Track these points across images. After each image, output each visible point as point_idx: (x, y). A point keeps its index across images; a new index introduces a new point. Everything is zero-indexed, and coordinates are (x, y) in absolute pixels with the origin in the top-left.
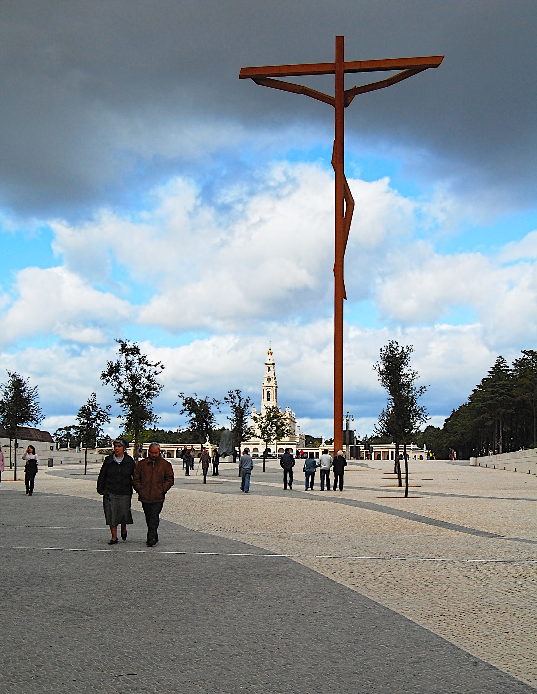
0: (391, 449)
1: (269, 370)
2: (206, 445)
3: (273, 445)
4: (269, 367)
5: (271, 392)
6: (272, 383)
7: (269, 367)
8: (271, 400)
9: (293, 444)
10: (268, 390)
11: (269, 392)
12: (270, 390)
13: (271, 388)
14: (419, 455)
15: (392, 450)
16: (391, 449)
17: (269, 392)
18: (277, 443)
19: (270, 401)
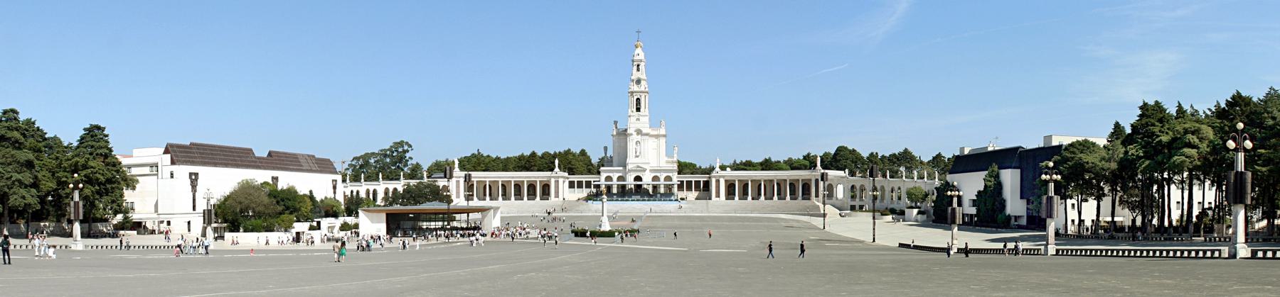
7: (638, 66)
10: (635, 98)
11: (638, 100)
12: (639, 97)
17: (638, 100)
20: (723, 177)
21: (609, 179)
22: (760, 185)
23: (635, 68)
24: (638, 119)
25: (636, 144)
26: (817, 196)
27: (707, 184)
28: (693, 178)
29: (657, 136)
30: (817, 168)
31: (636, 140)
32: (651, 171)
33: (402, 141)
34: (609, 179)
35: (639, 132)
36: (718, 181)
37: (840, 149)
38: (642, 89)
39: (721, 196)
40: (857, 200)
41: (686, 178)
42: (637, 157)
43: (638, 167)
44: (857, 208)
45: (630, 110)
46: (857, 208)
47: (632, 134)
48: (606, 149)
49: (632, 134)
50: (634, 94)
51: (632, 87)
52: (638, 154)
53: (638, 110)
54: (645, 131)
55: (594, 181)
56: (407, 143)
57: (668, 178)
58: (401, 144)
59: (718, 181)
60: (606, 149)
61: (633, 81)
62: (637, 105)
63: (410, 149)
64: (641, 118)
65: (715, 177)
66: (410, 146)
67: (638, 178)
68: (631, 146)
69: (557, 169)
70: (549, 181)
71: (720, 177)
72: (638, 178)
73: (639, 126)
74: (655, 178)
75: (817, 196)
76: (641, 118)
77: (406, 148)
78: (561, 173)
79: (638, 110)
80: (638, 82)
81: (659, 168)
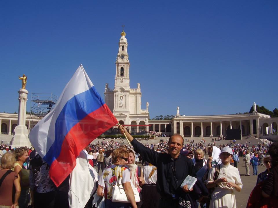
7: (123, 47)
12: (123, 66)
13: (124, 64)
19: (123, 76)
20: (183, 120)
23: (120, 48)
24: (122, 82)
25: (120, 98)
26: (255, 132)
29: (135, 94)
30: (254, 112)
32: (131, 117)
35: (123, 90)
36: (178, 124)
38: (125, 61)
42: (121, 107)
43: (122, 114)
45: (116, 75)
47: (117, 92)
50: (120, 64)
51: (118, 60)
52: (121, 105)
53: (122, 75)
54: (126, 90)
57: (142, 123)
61: (119, 56)
62: (121, 72)
64: (124, 80)
65: (176, 120)
68: (117, 100)
71: (180, 120)
73: (122, 85)
74: (134, 123)
75: (255, 132)
76: (124, 80)
80: (123, 57)
81: (136, 116)
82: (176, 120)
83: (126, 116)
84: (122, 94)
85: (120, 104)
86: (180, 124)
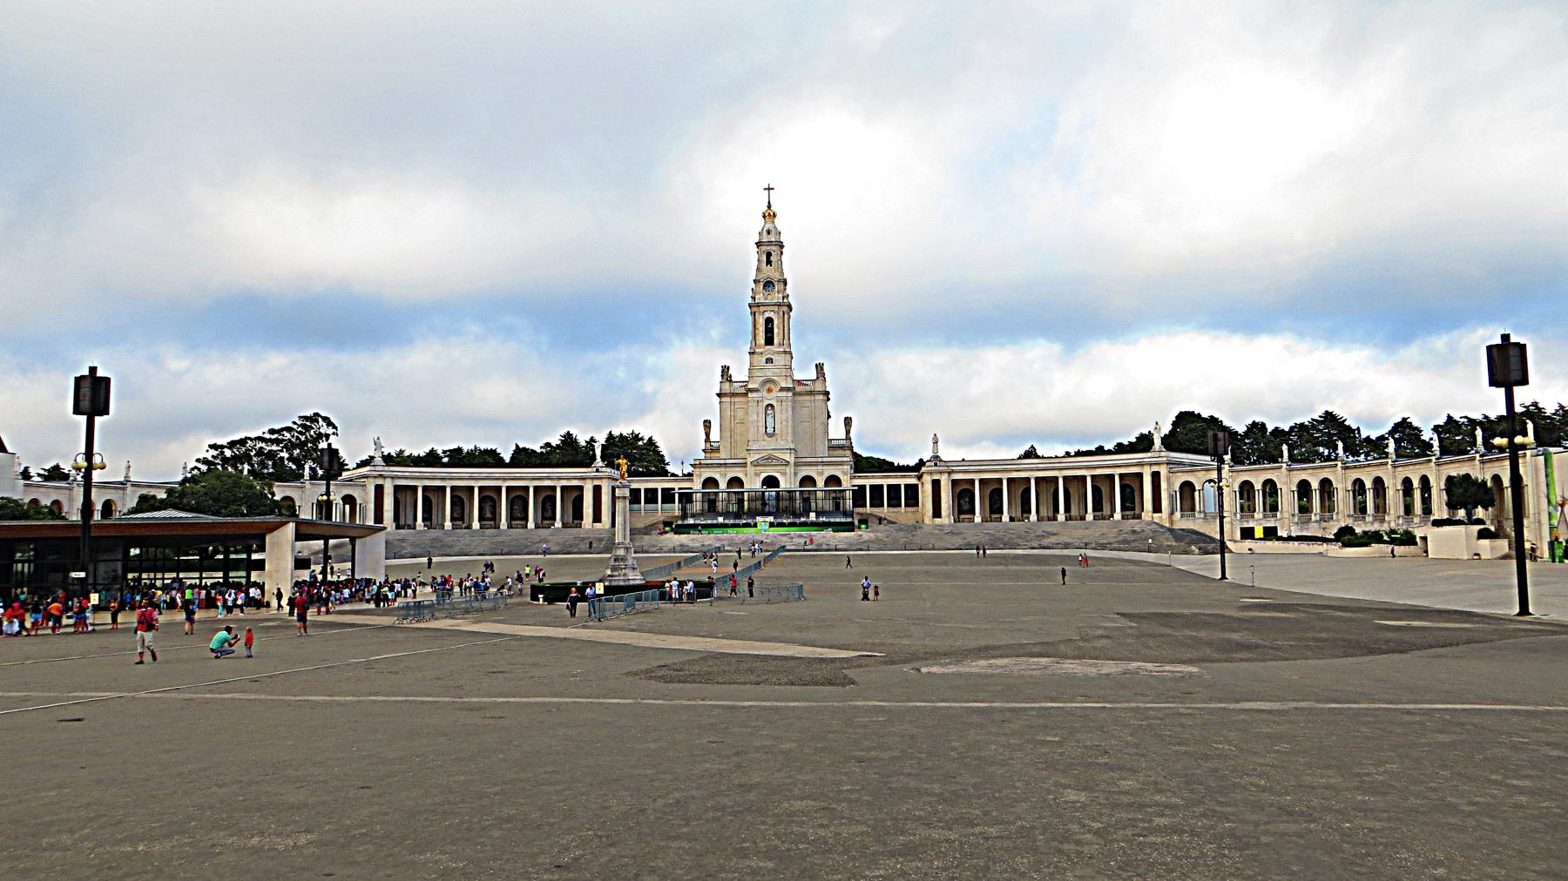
0: (1151, 464)
1: (769, 262)
2: (595, 469)
3: (784, 467)
4: (769, 255)
5: (776, 323)
6: (776, 297)
7: (769, 255)
8: (776, 341)
9: (842, 463)
10: (767, 315)
11: (769, 321)
12: (771, 315)
13: (776, 308)
14: (1296, 481)
15: (1155, 469)
16: (1151, 464)
17: (769, 321)
18: (796, 464)
19: (772, 344)
21: (710, 482)
22: (1028, 490)
24: (769, 361)
25: (768, 406)
27: (912, 491)
28: (885, 481)
31: (767, 402)
33: (317, 415)
34: (710, 482)
36: (936, 485)
37: (1184, 418)
39: (944, 513)
40: (1258, 515)
41: (868, 481)
42: (771, 436)
44: (1259, 533)
46: (1259, 533)
48: (707, 424)
49: (756, 390)
52: (770, 430)
53: (769, 341)
55: (680, 489)
56: (326, 419)
58: (314, 418)
59: (936, 485)
60: (707, 424)
63: (330, 431)
65: (931, 473)
66: (330, 423)
67: (771, 482)
69: (599, 462)
70: (581, 488)
72: (771, 482)
75: (1157, 508)
77: (324, 429)
78: (609, 470)
79: (769, 341)
82: (931, 473)
83: (788, 463)
84: (770, 398)
85: (766, 428)
86: (942, 483)
